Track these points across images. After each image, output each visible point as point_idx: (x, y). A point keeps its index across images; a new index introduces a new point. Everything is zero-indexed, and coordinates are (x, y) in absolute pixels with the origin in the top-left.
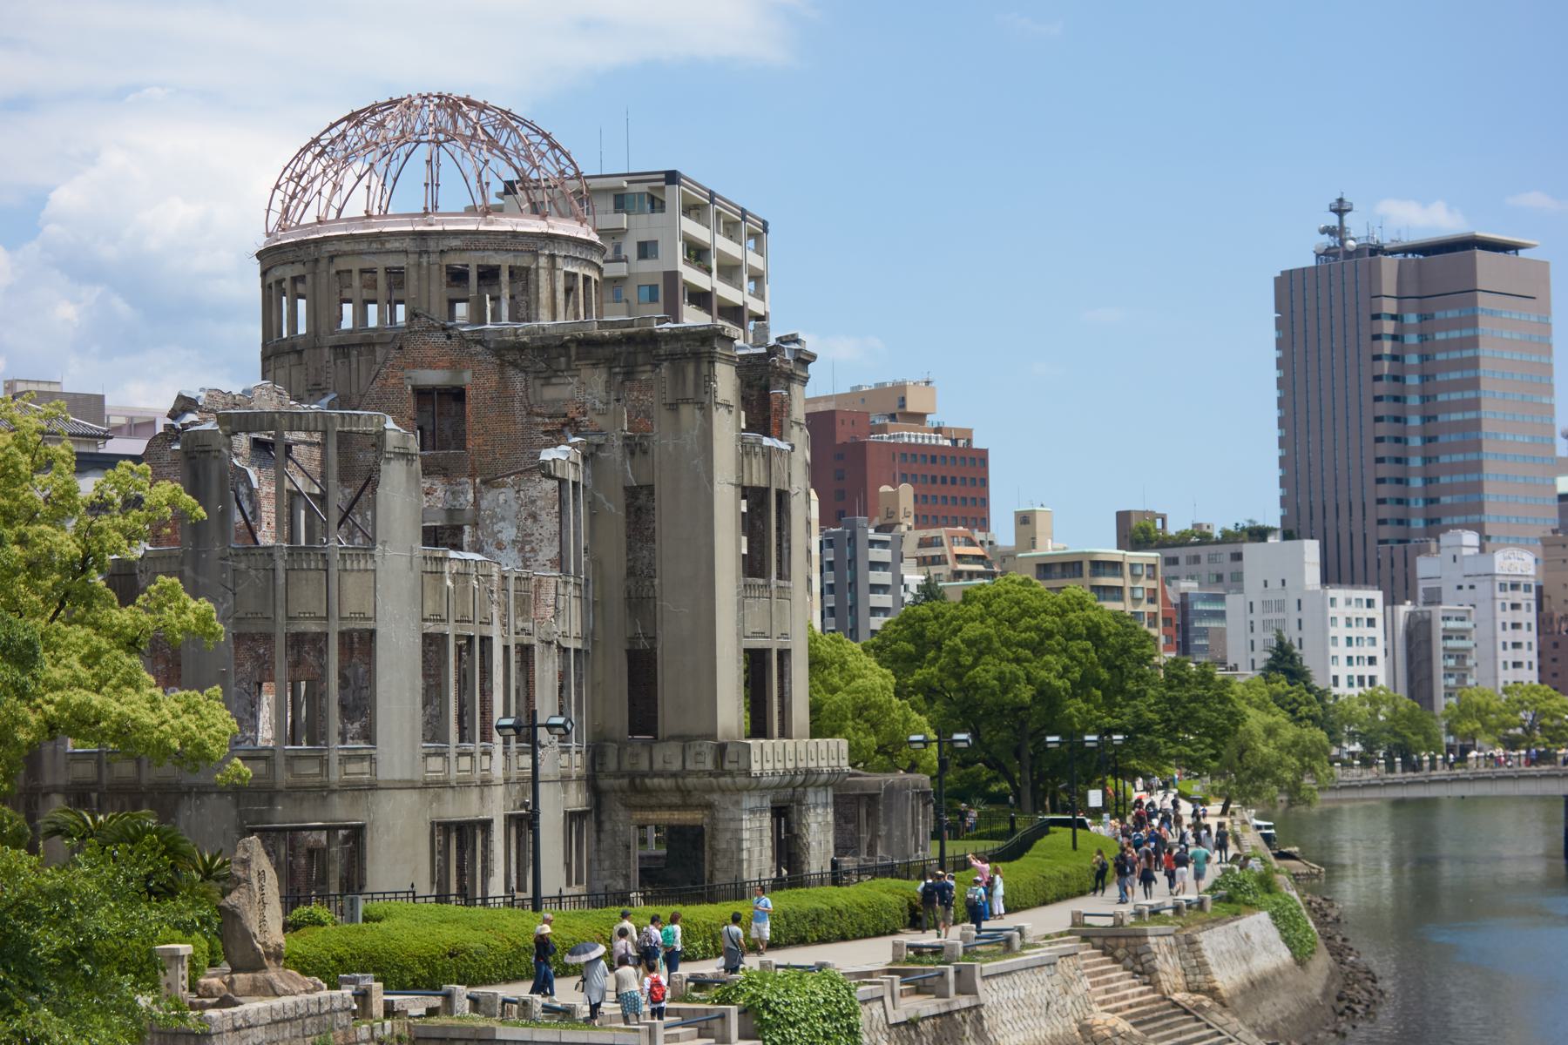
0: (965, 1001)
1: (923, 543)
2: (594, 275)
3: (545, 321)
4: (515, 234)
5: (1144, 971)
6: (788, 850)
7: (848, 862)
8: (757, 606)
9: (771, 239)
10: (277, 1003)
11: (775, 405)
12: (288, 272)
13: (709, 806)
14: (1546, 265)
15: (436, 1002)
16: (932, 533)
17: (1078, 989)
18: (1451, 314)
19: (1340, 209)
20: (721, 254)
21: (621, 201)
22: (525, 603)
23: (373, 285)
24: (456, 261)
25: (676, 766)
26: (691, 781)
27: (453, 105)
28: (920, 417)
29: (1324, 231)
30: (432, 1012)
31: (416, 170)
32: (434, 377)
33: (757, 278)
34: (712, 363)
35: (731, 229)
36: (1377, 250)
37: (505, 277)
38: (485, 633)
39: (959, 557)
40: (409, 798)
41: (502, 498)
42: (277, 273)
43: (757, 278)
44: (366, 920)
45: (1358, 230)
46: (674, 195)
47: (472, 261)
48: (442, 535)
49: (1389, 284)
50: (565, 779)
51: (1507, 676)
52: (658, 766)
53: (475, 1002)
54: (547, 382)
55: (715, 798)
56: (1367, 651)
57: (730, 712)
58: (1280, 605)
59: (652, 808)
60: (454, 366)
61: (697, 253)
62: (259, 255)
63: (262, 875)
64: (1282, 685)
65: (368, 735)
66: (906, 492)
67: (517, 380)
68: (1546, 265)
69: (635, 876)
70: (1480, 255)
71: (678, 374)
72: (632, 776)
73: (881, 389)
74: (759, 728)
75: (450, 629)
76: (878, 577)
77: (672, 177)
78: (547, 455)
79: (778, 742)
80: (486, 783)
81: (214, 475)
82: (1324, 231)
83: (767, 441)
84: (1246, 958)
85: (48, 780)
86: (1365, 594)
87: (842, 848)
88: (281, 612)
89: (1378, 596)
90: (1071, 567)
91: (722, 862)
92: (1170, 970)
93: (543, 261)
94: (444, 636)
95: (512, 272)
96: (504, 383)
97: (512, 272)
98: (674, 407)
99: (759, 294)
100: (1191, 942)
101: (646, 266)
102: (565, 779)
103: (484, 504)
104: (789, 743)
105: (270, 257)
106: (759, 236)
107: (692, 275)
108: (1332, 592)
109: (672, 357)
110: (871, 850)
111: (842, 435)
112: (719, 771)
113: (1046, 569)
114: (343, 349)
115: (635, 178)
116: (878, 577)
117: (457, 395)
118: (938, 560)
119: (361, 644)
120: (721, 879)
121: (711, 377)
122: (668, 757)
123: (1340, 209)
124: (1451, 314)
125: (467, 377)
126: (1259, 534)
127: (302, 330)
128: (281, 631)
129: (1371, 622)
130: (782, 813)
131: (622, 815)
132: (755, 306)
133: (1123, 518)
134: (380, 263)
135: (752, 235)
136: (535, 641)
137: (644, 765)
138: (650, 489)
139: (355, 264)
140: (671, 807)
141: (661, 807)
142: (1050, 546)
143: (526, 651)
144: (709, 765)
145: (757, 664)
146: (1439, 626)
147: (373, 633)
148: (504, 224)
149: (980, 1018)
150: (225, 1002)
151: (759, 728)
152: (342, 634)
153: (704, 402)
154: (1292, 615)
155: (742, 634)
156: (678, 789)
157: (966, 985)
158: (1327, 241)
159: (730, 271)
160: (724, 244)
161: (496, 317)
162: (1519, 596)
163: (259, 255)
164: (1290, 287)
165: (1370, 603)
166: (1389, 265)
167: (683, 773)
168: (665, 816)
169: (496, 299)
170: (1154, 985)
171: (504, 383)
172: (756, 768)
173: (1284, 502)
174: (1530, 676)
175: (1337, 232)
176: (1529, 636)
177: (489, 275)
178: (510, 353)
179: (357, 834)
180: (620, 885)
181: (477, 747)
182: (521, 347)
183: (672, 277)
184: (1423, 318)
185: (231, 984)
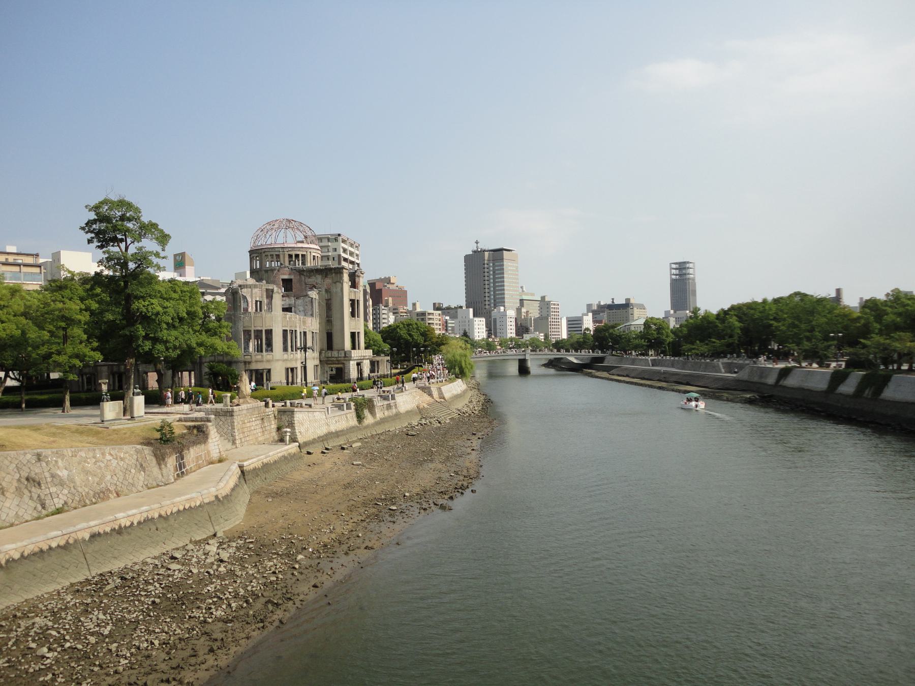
0: (393, 401)
1: (394, 309)
2: (319, 256)
3: (309, 265)
4: (302, 248)
5: (430, 394)
6: (360, 371)
7: (372, 375)
8: (353, 323)
10: (248, 405)
11: (357, 282)
12: (255, 255)
13: (344, 364)
15: (283, 404)
17: (416, 399)
19: (477, 243)
20: (350, 251)
21: (329, 240)
22: (304, 322)
23: (272, 258)
24: (290, 253)
25: (337, 356)
27: (289, 221)
28: (393, 284)
30: (283, 406)
31: (282, 234)
32: (286, 277)
33: (357, 255)
35: (352, 245)
36: (484, 251)
37: (300, 256)
39: (402, 312)
40: (280, 363)
41: (299, 302)
42: (252, 256)
44: (271, 389)
45: (481, 246)
46: (340, 239)
47: (293, 253)
48: (287, 309)
49: (486, 258)
51: (509, 336)
52: (333, 356)
53: (291, 403)
54: (309, 278)
55: (345, 362)
58: (465, 322)
59: (331, 364)
60: (290, 274)
61: (345, 250)
63: (245, 379)
64: (464, 338)
65: (272, 351)
66: (390, 299)
67: (303, 277)
69: (329, 378)
70: (504, 252)
73: (385, 278)
74: (354, 348)
75: (288, 329)
76: (384, 316)
77: (339, 235)
78: (309, 293)
79: (357, 351)
80: (296, 360)
81: (238, 297)
83: (355, 290)
84: (451, 392)
85: (204, 361)
87: (372, 371)
88: (253, 326)
89: (484, 319)
90: (423, 314)
91: (346, 375)
93: (309, 253)
94: (286, 331)
95: (302, 255)
97: (302, 255)
98: (335, 283)
99: (358, 259)
100: (440, 388)
102: (314, 359)
103: (297, 303)
105: (252, 252)
107: (343, 255)
108: (475, 319)
109: (335, 273)
110: (378, 372)
111: (377, 288)
112: (345, 356)
113: (418, 314)
114: (266, 271)
115: (332, 235)
116: (384, 316)
117: (290, 280)
119: (269, 332)
120: (346, 378)
122: (335, 354)
123: (477, 243)
125: (292, 277)
126: (461, 307)
127: (258, 267)
128: (253, 329)
130: (358, 364)
131: (326, 365)
132: (357, 261)
133: (434, 304)
134: (274, 253)
135: (356, 247)
136: (307, 331)
137: (330, 356)
138: (330, 299)
139: (269, 254)
140: (336, 364)
141: (334, 364)
142: (419, 310)
143: (305, 333)
144: (343, 355)
145: (353, 335)
147: (271, 330)
148: (300, 245)
149: (396, 405)
150: (238, 405)
151: (354, 348)
152: (266, 330)
153: (341, 281)
154: (467, 323)
156: (337, 360)
157: (393, 398)
158: (475, 249)
159: (351, 254)
160: (350, 249)
161: (299, 265)
162: (512, 320)
164: (467, 258)
166: (486, 254)
168: (335, 366)
169: (298, 261)
170: (433, 398)
172: (353, 355)
173: (466, 301)
174: (514, 335)
176: (514, 327)
177: (297, 256)
178: (301, 272)
179: (269, 371)
180: (326, 380)
181: (294, 352)
182: (303, 271)
183: (339, 256)
184: (493, 264)
185: (239, 401)
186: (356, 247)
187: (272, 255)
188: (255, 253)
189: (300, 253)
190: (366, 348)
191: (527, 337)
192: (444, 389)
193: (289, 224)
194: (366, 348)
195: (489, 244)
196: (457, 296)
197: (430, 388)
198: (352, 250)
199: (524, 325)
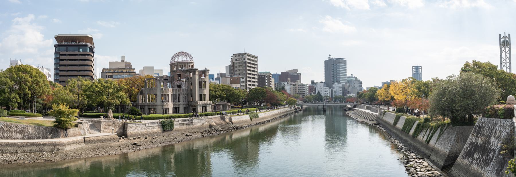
0: (191, 122)
1: (291, 83)
9: (258, 58)
13: (196, 106)
14: (346, 61)
16: (292, 82)
18: (338, 64)
24: (180, 64)
26: (194, 104)
29: (328, 57)
32: (179, 74)
33: (256, 61)
34: (195, 72)
35: (253, 57)
38: (168, 94)
39: (294, 84)
43: (257, 61)
45: (331, 57)
47: (181, 64)
50: (184, 104)
51: (339, 95)
56: (327, 93)
57: (197, 98)
60: (180, 73)
61: (249, 59)
62: (170, 64)
68: (346, 61)
71: (193, 72)
72: (191, 104)
77: (246, 53)
82: (328, 57)
83: (202, 77)
86: (327, 88)
89: (328, 88)
92: (227, 120)
96: (183, 74)
101: (244, 61)
104: (204, 102)
106: (257, 58)
118: (292, 85)
121: (195, 73)
124: (338, 64)
125: (181, 73)
129: (328, 90)
132: (257, 64)
141: (193, 106)
144: (195, 103)
146: (334, 90)
154: (321, 89)
155: (199, 93)
158: (329, 58)
159: (253, 61)
162: (341, 88)
163: (170, 64)
164: (326, 62)
165: (328, 88)
167: (194, 104)
170: (225, 121)
171: (183, 74)
175: (330, 57)
183: (246, 61)
186: (256, 57)
187: (174, 66)
188: (172, 65)
189: (184, 64)
190: (210, 100)
191: (348, 95)
192: (233, 118)
193: (184, 54)
194: (210, 100)
195: (334, 56)
196: (320, 77)
197: (224, 117)
198: (253, 59)
199: (348, 90)
